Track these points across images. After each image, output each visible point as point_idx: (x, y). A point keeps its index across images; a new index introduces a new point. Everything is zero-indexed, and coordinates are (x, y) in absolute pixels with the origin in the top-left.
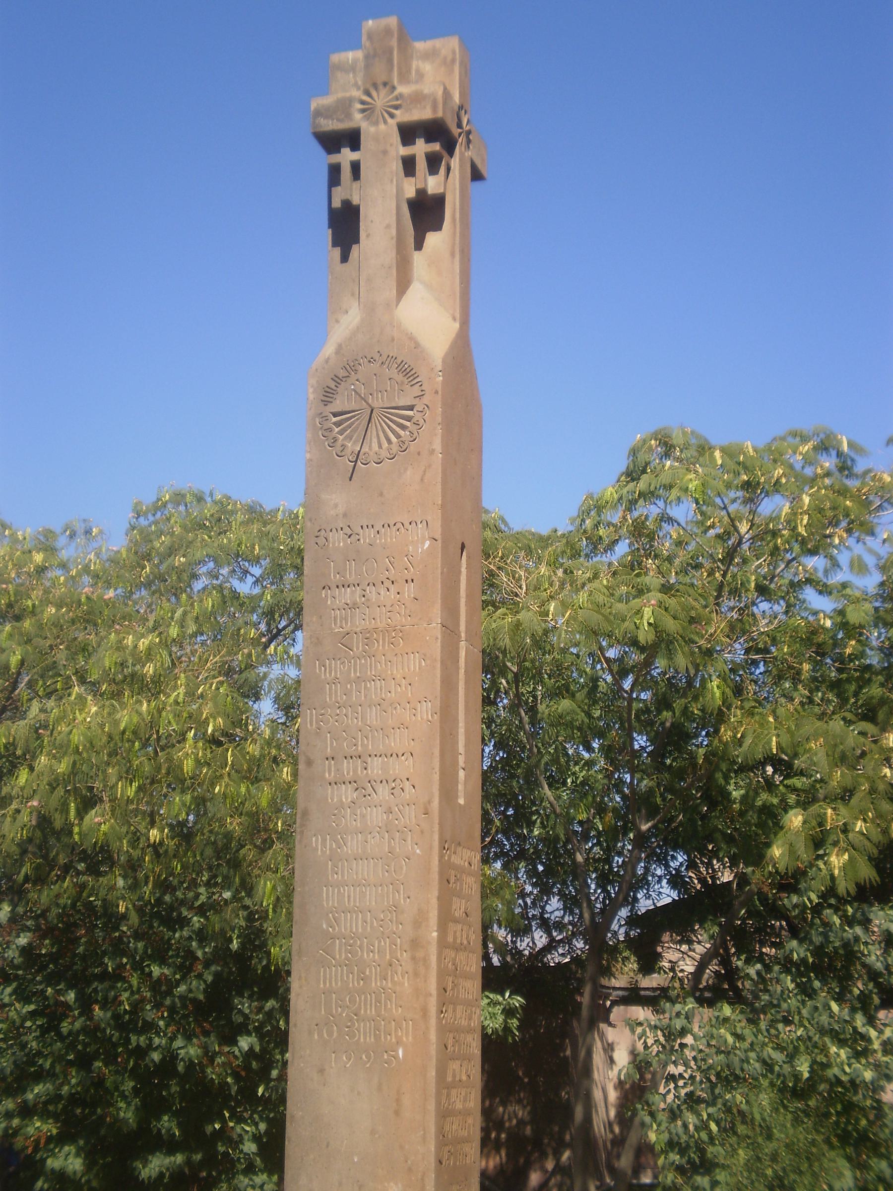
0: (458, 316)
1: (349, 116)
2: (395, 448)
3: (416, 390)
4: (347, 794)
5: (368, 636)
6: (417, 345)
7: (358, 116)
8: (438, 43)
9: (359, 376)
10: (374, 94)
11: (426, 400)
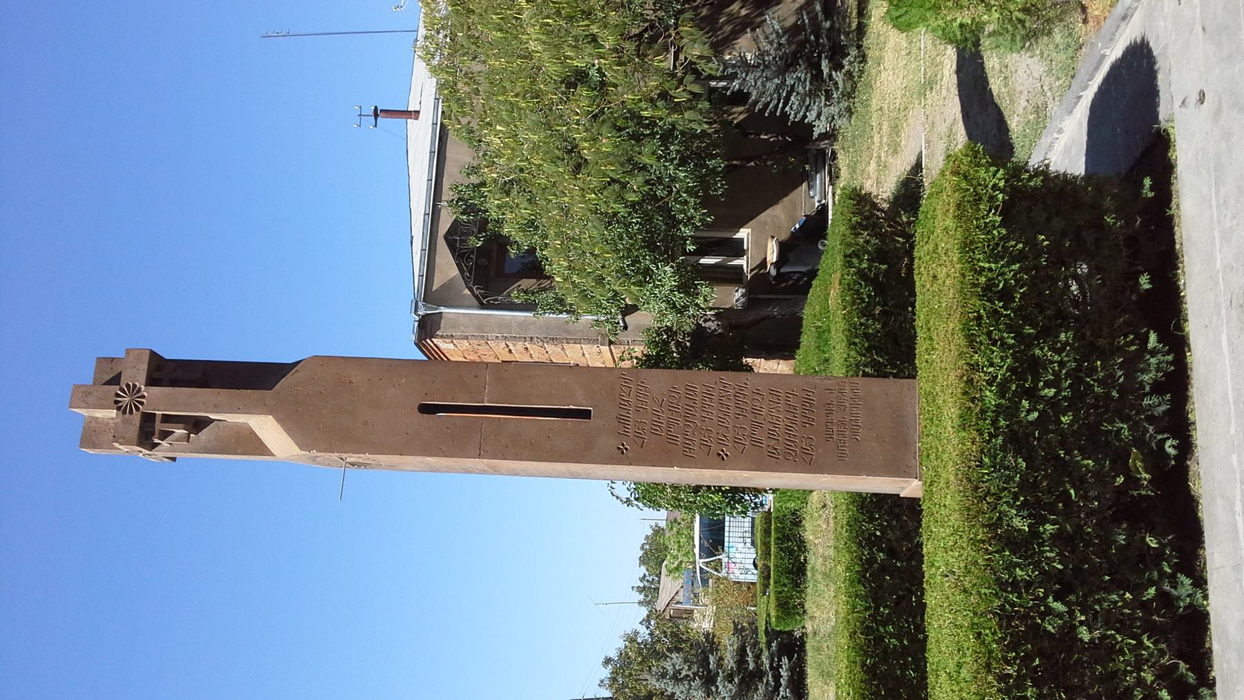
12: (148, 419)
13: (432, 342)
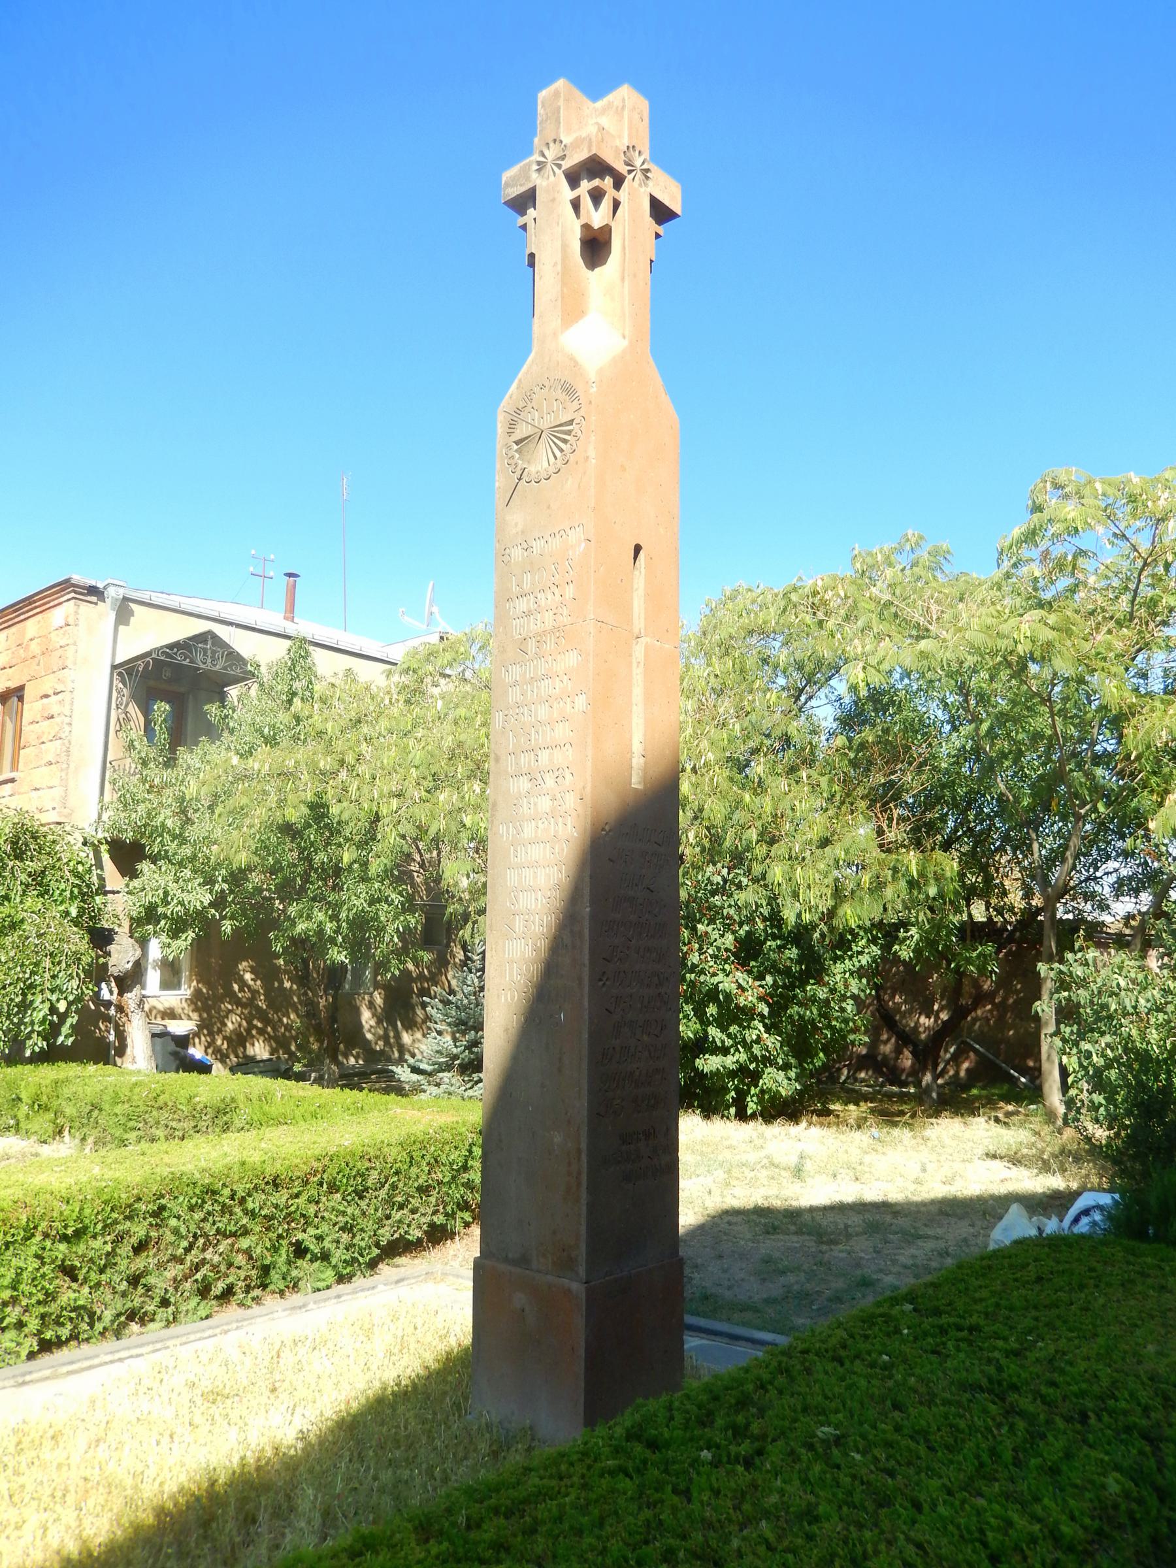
0: (627, 333)
1: (528, 178)
2: (559, 462)
3: (575, 405)
4: (524, 784)
5: (540, 640)
6: (576, 364)
7: (534, 175)
8: (610, 97)
9: (534, 404)
10: (546, 153)
11: (582, 413)
12: (618, 182)
13: (69, 600)
